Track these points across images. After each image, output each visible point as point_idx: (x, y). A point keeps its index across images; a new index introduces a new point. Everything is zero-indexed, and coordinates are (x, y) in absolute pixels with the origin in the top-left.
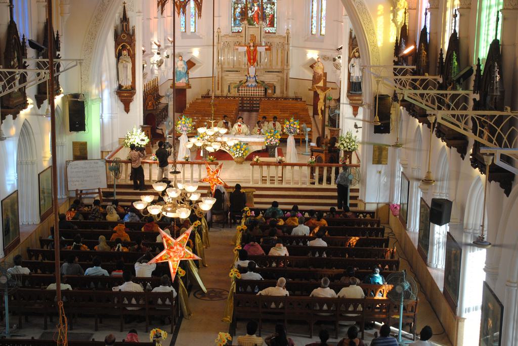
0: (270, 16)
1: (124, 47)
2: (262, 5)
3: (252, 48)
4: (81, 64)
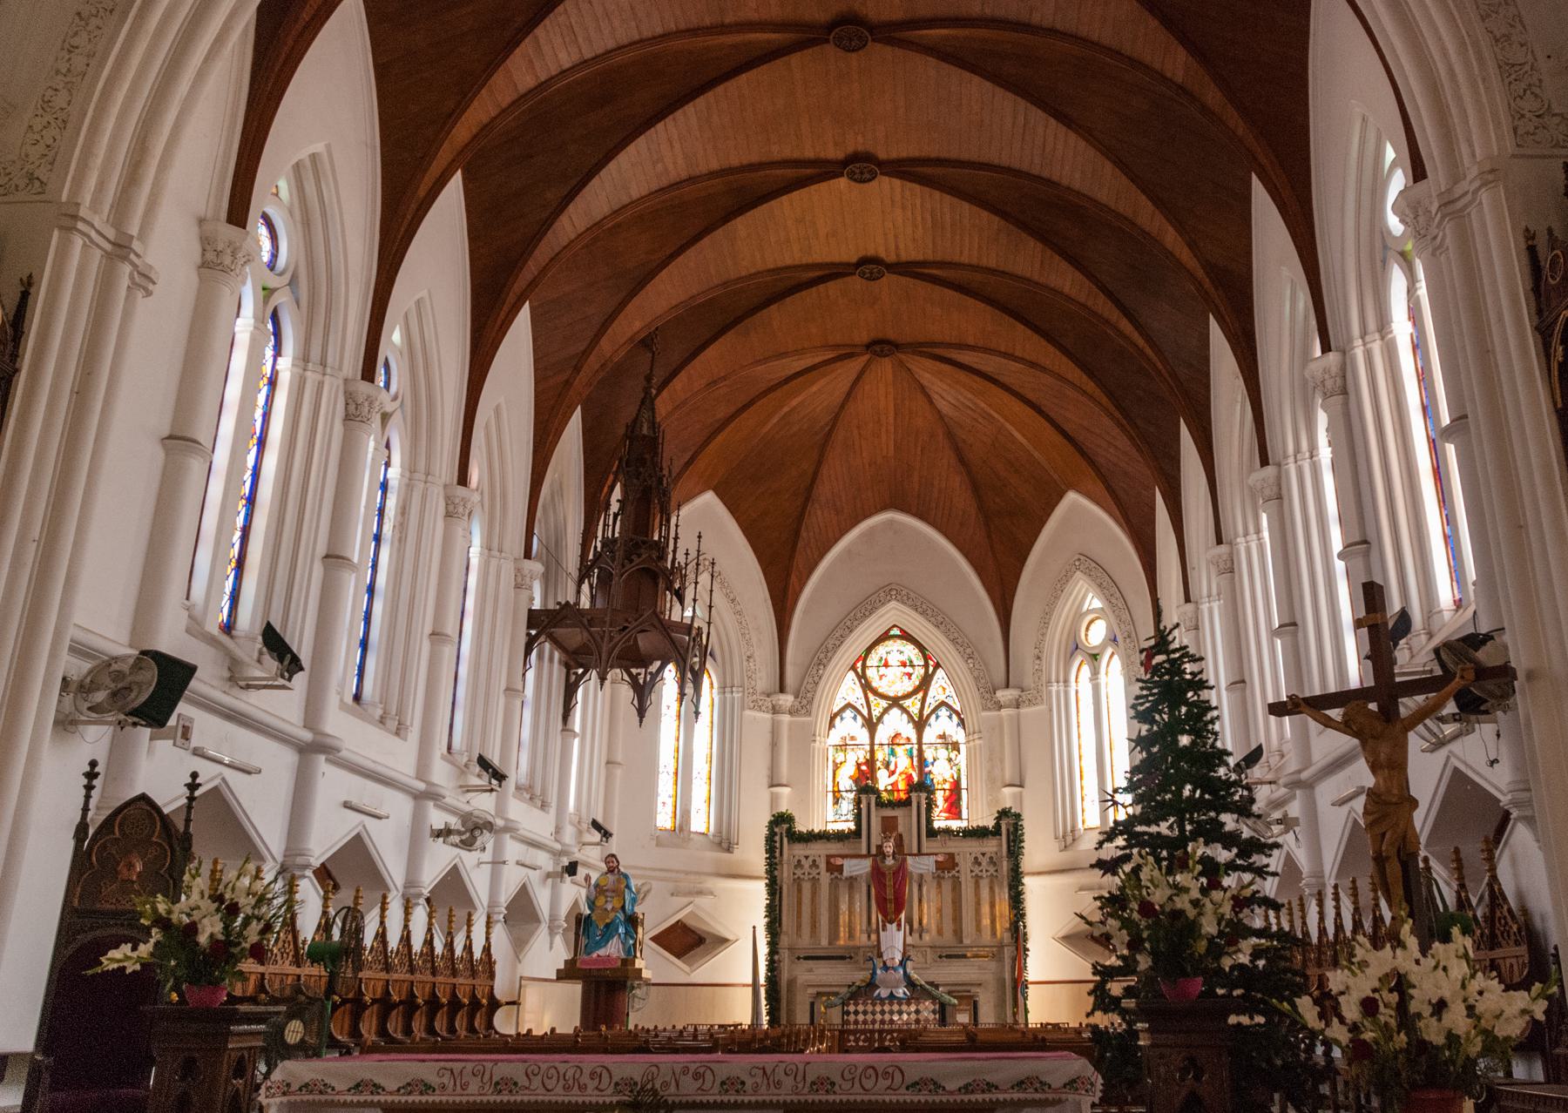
0: (947, 786)
2: (920, 751)
3: (890, 862)
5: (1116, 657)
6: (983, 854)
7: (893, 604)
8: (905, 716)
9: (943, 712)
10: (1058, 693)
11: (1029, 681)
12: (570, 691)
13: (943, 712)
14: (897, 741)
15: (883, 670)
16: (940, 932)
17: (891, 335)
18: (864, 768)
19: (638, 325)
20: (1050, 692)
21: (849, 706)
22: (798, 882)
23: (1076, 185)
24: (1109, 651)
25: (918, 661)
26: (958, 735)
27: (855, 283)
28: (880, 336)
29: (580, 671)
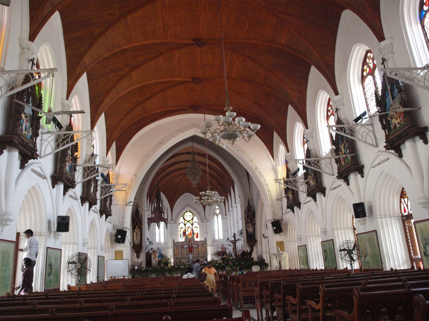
0: (196, 234)
1: (137, 224)
2: (192, 229)
4: (126, 186)
16: (196, 254)
18: (184, 231)
25: (192, 215)
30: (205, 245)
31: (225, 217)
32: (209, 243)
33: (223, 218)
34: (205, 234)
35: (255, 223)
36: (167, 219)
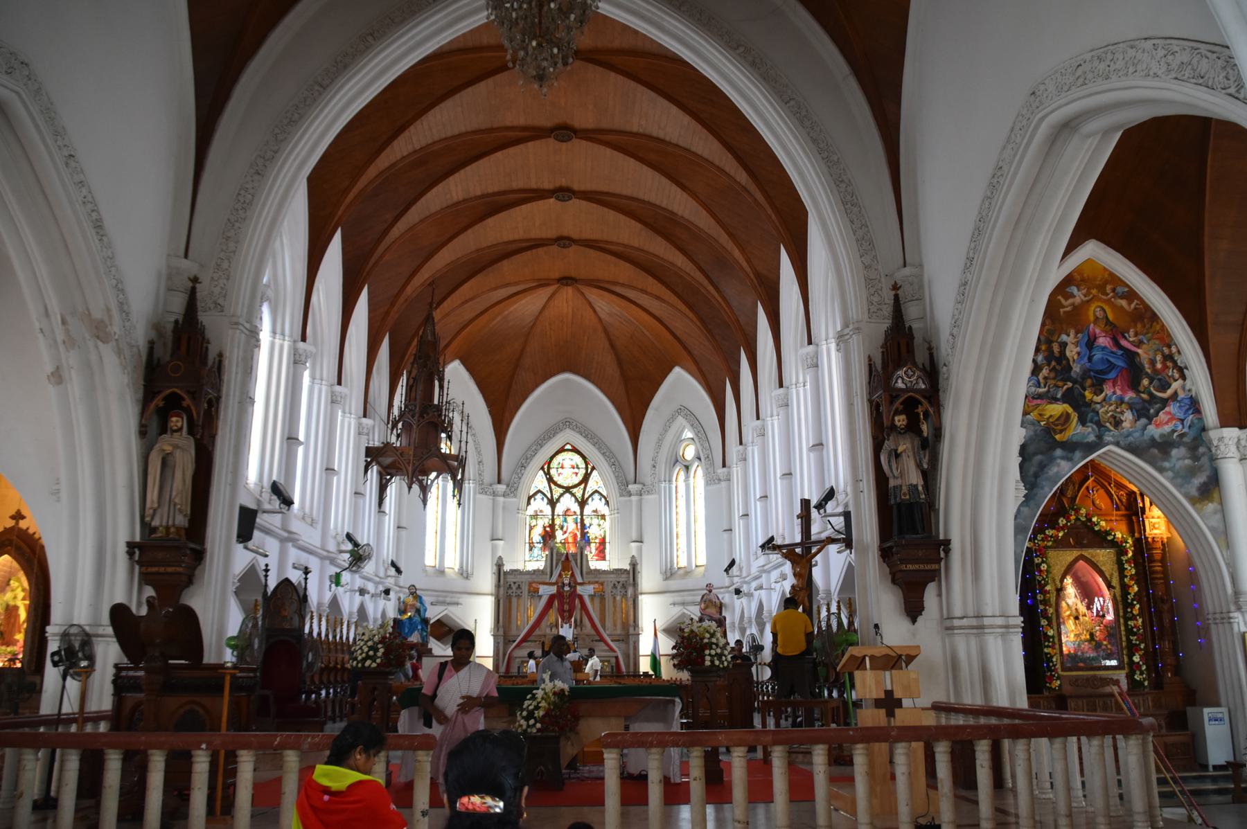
0: (597, 541)
2: (582, 520)
3: (567, 588)
5: (700, 468)
6: (619, 582)
7: (568, 430)
8: (573, 499)
9: (596, 496)
10: (665, 487)
11: (648, 480)
12: (382, 489)
13: (596, 496)
14: (568, 513)
15: (560, 470)
17: (573, 274)
18: (548, 529)
19: (426, 276)
20: (659, 487)
21: (539, 491)
22: (509, 598)
23: (686, 216)
24: (696, 464)
25: (582, 465)
26: (604, 510)
27: (554, 249)
28: (567, 274)
29: (388, 477)
30: (630, 591)
31: (721, 471)
32: (649, 579)
33: (711, 480)
34: (634, 545)
35: (938, 433)
36: (461, 461)
